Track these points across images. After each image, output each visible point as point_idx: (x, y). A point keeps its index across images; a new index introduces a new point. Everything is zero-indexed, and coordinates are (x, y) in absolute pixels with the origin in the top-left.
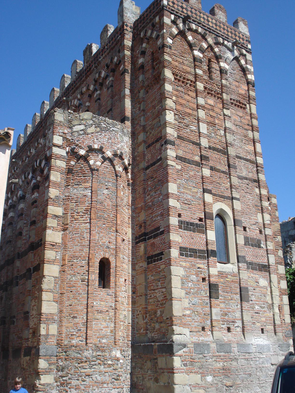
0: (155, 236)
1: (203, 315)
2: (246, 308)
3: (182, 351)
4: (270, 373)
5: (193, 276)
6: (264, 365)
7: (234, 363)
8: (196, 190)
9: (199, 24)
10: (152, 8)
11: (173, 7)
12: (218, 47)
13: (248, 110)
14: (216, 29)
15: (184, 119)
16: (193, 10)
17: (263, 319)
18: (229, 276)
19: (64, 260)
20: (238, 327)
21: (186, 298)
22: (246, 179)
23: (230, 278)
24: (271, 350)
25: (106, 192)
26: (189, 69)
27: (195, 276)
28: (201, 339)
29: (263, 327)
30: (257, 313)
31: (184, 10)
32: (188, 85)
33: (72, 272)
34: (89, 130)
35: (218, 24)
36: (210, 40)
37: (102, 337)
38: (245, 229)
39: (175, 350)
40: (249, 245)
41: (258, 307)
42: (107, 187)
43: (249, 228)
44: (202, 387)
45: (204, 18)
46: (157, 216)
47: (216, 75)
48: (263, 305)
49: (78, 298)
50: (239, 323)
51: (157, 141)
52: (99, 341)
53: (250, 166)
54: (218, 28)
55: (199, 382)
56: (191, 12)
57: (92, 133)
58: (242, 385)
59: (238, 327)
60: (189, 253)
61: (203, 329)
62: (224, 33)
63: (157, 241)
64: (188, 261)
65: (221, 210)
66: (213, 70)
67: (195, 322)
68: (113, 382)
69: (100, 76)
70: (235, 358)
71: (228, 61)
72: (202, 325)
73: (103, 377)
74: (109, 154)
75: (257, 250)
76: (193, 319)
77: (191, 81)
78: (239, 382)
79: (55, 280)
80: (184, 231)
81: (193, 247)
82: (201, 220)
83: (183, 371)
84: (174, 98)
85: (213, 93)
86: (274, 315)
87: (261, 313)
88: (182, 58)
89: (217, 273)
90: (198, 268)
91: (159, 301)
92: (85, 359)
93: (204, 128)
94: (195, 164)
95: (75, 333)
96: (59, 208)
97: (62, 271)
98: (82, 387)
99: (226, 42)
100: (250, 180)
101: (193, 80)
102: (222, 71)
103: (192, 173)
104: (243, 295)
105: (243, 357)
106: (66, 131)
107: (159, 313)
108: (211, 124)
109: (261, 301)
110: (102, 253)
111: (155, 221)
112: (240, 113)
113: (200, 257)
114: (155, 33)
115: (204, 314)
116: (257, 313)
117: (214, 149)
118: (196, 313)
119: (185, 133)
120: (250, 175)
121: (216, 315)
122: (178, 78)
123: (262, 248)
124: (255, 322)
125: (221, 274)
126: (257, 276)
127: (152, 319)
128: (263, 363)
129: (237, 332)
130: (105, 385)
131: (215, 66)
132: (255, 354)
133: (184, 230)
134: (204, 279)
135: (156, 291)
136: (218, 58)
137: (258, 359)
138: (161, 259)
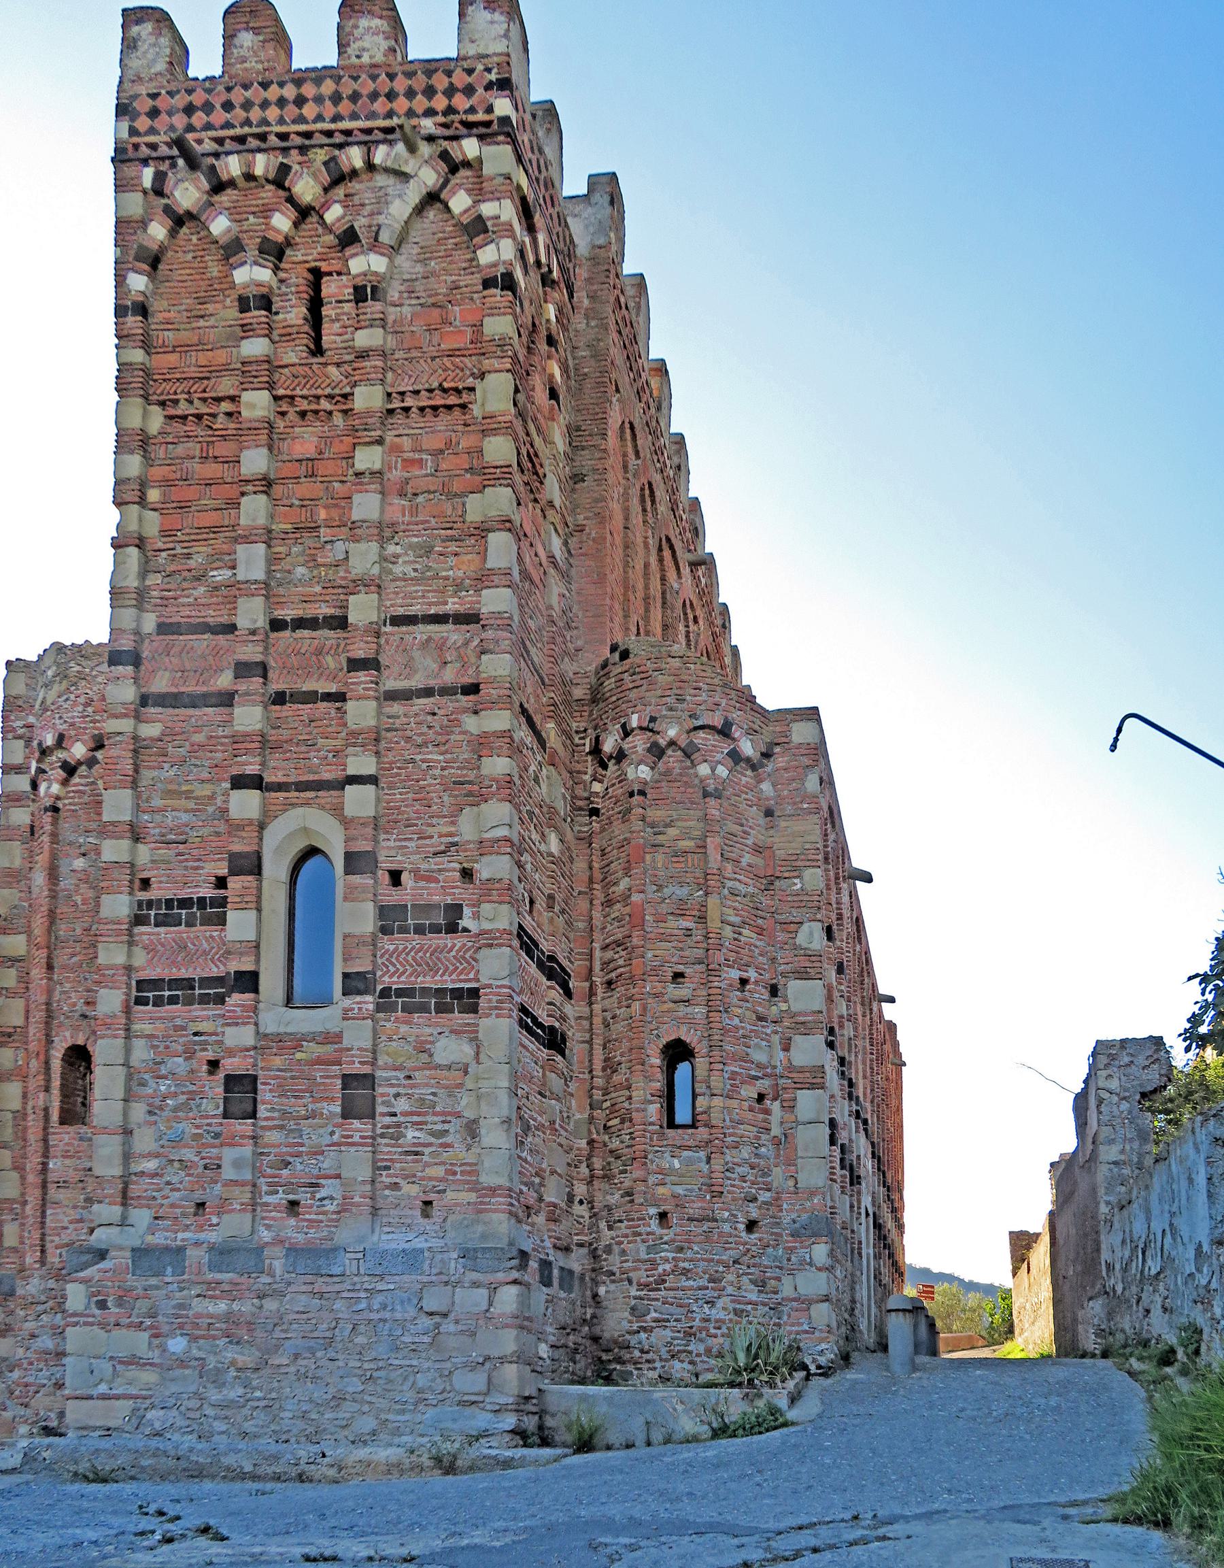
1: (200, 1170)
2: (356, 1139)
4: (408, 1339)
5: (176, 1059)
6: (387, 1315)
7: (270, 1305)
8: (206, 790)
17: (439, 1171)
22: (428, 692)
24: (426, 1267)
27: (180, 1060)
28: (180, 1235)
29: (432, 1196)
30: (416, 1153)
38: (396, 877)
40: (404, 930)
41: (417, 1134)
43: (417, 875)
44: (151, 1364)
48: (439, 1127)
55: (143, 1350)
58: (292, 1369)
60: (167, 993)
64: (160, 1018)
67: (172, 1190)
70: (274, 1291)
72: (198, 1196)
75: (445, 940)
76: (168, 1183)
80: (158, 929)
81: (184, 973)
82: (221, 883)
83: (90, 1319)
87: (427, 1151)
88: (202, 323)
90: (195, 1034)
94: (213, 700)
100: (446, 691)
105: (304, 1288)
109: (435, 1114)
113: (204, 1000)
115: (206, 1168)
116: (416, 1153)
118: (176, 1165)
121: (237, 1164)
123: (465, 930)
124: (397, 1180)
125: (268, 1043)
126: (428, 1030)
128: (384, 1307)
132: (356, 1279)
133: (156, 925)
137: (363, 1295)
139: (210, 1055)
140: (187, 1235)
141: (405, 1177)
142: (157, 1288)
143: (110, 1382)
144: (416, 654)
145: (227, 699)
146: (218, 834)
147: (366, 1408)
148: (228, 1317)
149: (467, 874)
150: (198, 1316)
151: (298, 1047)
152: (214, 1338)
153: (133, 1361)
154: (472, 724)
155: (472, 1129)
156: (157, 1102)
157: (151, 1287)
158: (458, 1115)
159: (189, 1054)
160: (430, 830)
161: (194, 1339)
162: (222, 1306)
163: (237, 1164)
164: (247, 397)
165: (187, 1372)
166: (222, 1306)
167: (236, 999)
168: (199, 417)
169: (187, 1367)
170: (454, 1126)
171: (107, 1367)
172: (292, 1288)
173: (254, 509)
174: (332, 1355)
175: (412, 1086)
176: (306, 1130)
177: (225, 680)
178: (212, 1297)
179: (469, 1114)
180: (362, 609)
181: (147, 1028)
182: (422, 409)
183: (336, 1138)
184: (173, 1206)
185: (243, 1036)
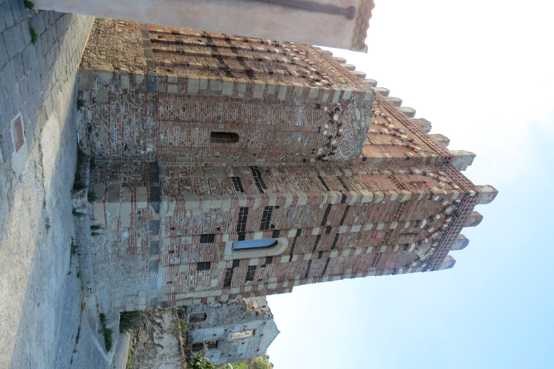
0: (258, 185)
2: (191, 268)
3: (153, 209)
6: (138, 284)
7: (140, 257)
8: (300, 222)
9: (451, 224)
10: (466, 181)
11: (468, 201)
12: (429, 242)
13: (370, 268)
14: (446, 240)
15: (365, 211)
16: (464, 219)
17: (180, 283)
18: (220, 252)
19: (237, 100)
20: (174, 260)
21: (202, 214)
22: (309, 267)
23: (219, 253)
25: (299, 139)
26: (410, 215)
28: (164, 227)
31: (464, 211)
32: (395, 215)
33: (226, 108)
34: (355, 124)
35: (450, 242)
36: (435, 235)
37: (166, 135)
38: (264, 266)
39: (153, 203)
40: (249, 270)
42: (303, 140)
44: (118, 228)
45: (456, 229)
46: (276, 186)
47: (404, 240)
48: (193, 282)
49: (202, 113)
50: (177, 261)
51: (345, 187)
52: (162, 132)
53: (321, 271)
54: (447, 242)
56: (463, 218)
57: (353, 127)
58: (119, 265)
59: (174, 260)
61: (173, 229)
62: (442, 247)
63: (254, 187)
65: (282, 245)
66: (408, 237)
68: (123, 145)
69: (401, 133)
71: (416, 251)
72: (177, 228)
73: (128, 134)
74: (334, 142)
75: (245, 277)
76: (182, 220)
77: (399, 218)
78: (121, 262)
79: (219, 91)
81: (248, 220)
82: (273, 226)
84: (384, 202)
85: (388, 237)
86: (184, 293)
87: (187, 281)
89: (223, 241)
91: (198, 188)
92: (145, 118)
93: (356, 229)
95: (169, 109)
96: (285, 96)
97: (226, 98)
98: (118, 116)
99: (433, 249)
100: (308, 271)
101: (400, 220)
102: (407, 246)
103: (315, 218)
104: (204, 266)
106: (355, 102)
107: (188, 188)
108: (359, 235)
110: (243, 135)
111: (272, 184)
112: (369, 262)
113: (239, 226)
114: (444, 185)
115: (186, 230)
117: (336, 239)
119: (352, 213)
120: (311, 271)
121: (186, 241)
122: (403, 206)
125: (223, 245)
126: (221, 278)
127: (181, 181)
129: (170, 260)
130: (120, 137)
131: (412, 238)
134: (219, 229)
135: (208, 185)
136: (419, 243)
138: (237, 190)
139: (222, 228)
140: (164, 228)
141: (179, 278)
142: (145, 227)
143: (111, 216)
144: (319, 264)
146: (287, 225)
147: (108, 283)
148: (135, 248)
150: (136, 240)
151: (220, 250)
152: (129, 245)
153: (119, 222)
155: (192, 290)
156: (209, 215)
157: (145, 227)
158: (196, 286)
159: (223, 223)
160: (274, 272)
161: (128, 239)
162: (139, 245)
163: (186, 241)
164: (397, 224)
165: (116, 238)
166: (139, 245)
167: (237, 236)
168: (398, 210)
169: (118, 238)
170: (193, 285)
171: (117, 216)
172: (145, 263)
174: (124, 273)
175: (205, 276)
176: (195, 254)
177: (328, 223)
178: (142, 243)
179: (196, 289)
181: (233, 211)
182: (376, 257)
183: (193, 261)
184: (174, 222)
185: (226, 238)
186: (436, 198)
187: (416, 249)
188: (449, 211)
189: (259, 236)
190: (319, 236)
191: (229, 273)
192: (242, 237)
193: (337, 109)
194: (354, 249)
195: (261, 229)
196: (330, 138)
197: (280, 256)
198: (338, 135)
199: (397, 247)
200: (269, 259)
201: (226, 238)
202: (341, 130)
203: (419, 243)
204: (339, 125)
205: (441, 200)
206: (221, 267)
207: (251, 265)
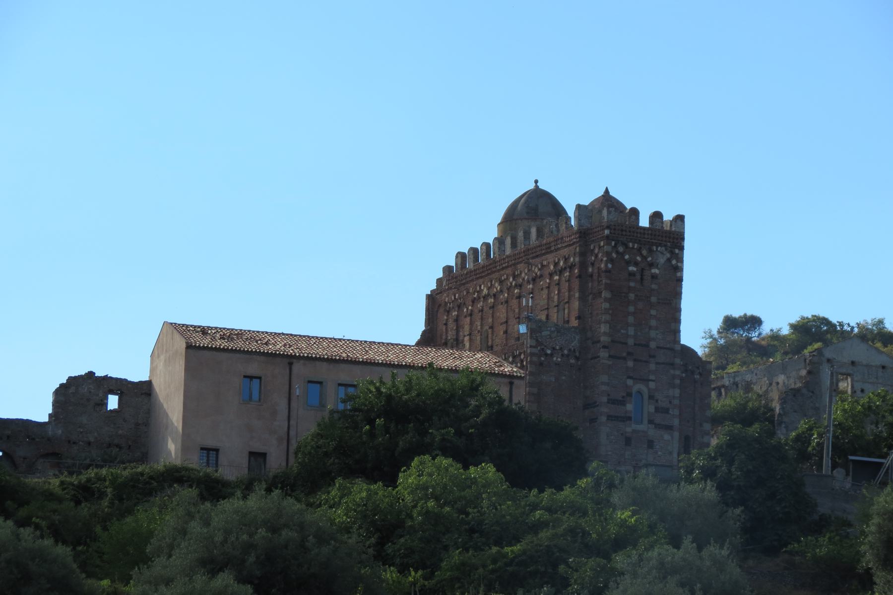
22: (663, 363)
36: (644, 252)
38: (657, 401)
82: (623, 397)
93: (631, 331)
102: (654, 277)
104: (650, 444)
117: (639, 345)
125: (634, 431)
145: (624, 359)
149: (670, 402)
154: (672, 372)
155: (671, 453)
173: (631, 319)
177: (624, 354)
180: (653, 345)
185: (629, 430)
186: (610, 266)
187: (657, 267)
188: (621, 249)
189: (629, 407)
190: (635, 360)
191: (658, 426)
192: (630, 418)
193: (543, 349)
194: (650, 328)
195: (624, 405)
196: (562, 355)
197: (649, 389)
198: (561, 349)
199: (653, 286)
200: (651, 397)
201: (629, 430)
202: (558, 348)
203: (651, 265)
204: (554, 349)
205: (611, 260)
206: (652, 432)
207: (653, 411)
